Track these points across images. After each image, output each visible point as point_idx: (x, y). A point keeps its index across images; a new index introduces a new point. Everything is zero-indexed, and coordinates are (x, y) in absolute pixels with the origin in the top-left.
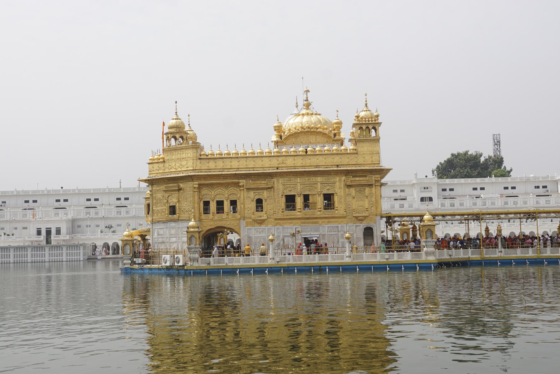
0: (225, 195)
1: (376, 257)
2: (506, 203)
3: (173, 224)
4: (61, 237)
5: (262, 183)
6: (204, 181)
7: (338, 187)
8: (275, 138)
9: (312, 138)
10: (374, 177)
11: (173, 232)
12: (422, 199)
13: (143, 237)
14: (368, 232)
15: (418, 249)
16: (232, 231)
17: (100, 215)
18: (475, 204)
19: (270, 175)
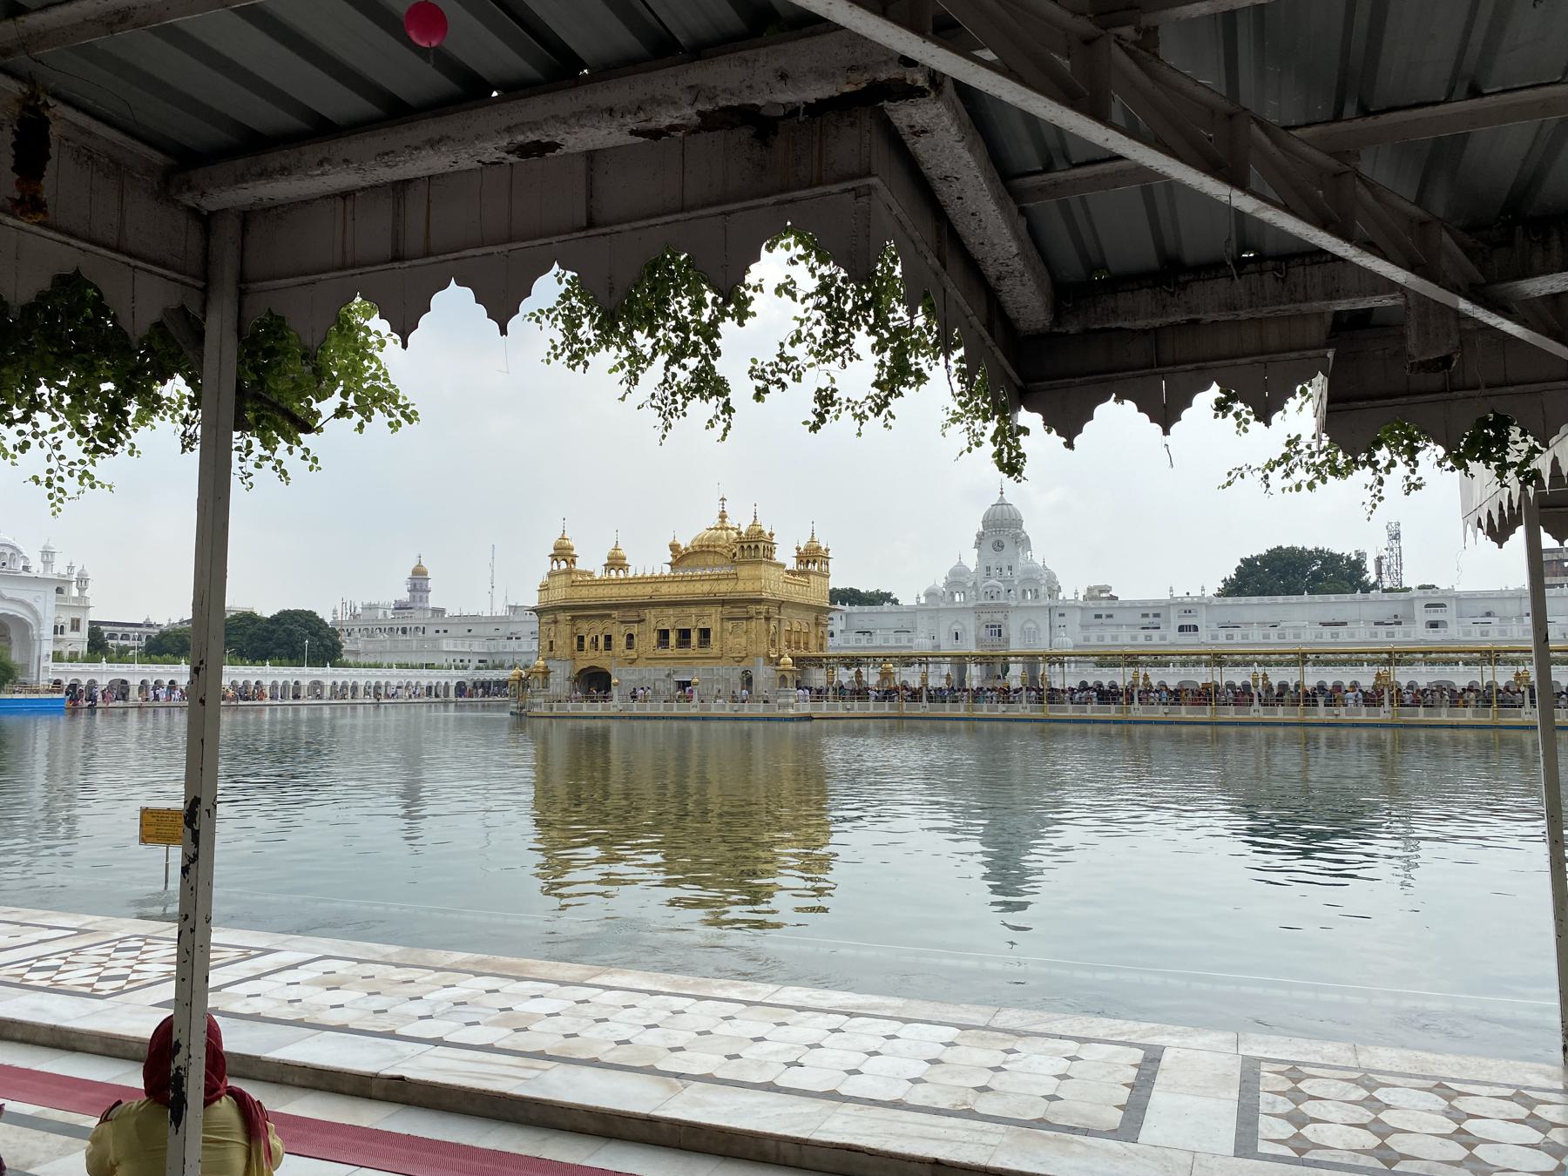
0: (598, 628)
1: (723, 707)
6: (578, 611)
8: (670, 559)
9: (710, 559)
10: (753, 609)
12: (1181, 629)
18: (1266, 637)
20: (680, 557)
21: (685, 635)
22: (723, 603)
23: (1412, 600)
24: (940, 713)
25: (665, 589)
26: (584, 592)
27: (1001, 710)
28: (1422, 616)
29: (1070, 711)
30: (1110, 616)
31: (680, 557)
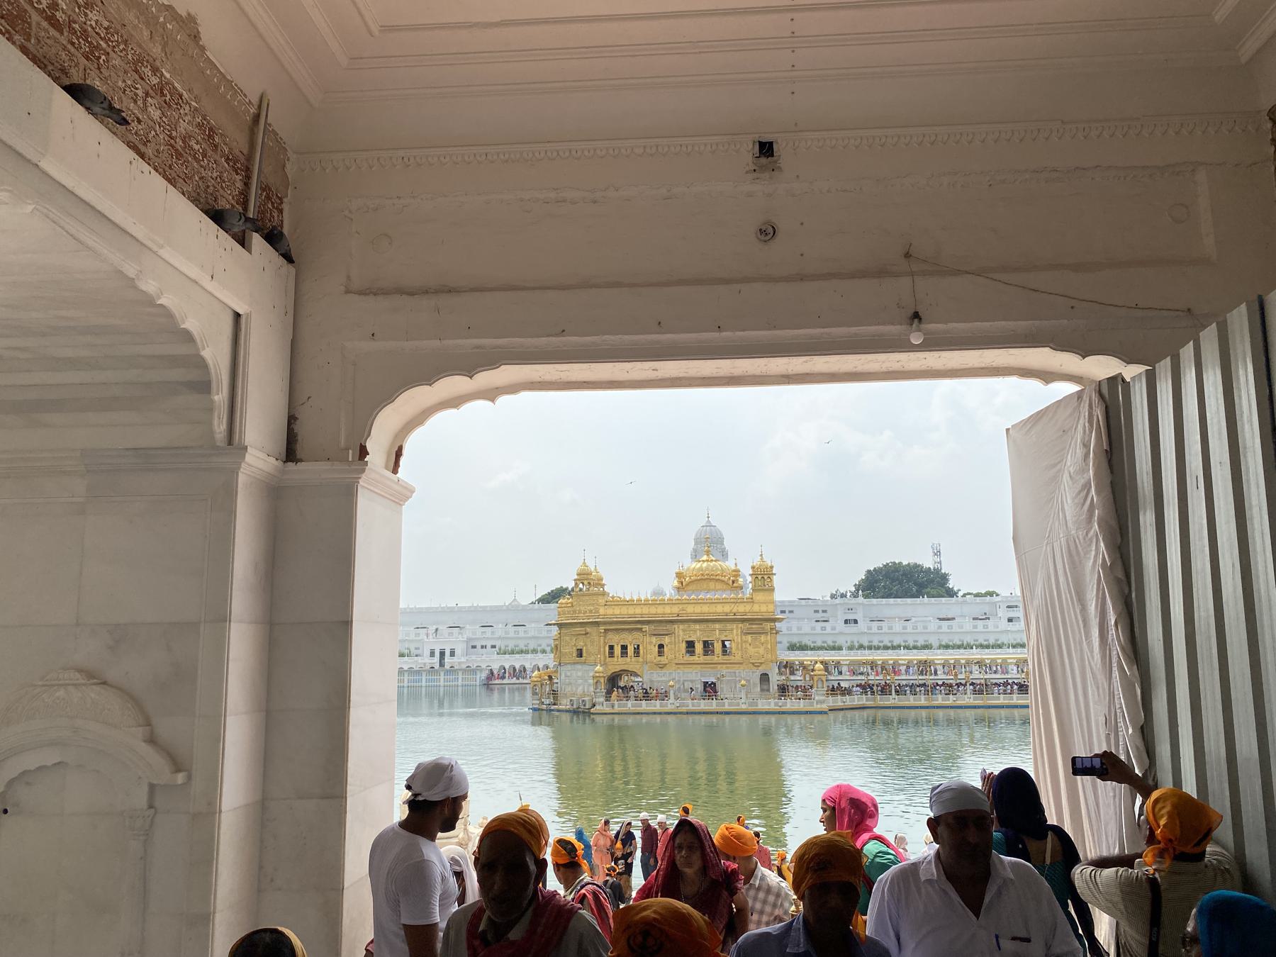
2: (940, 627)
3: (579, 667)
4: (455, 659)
5: (662, 629)
7: (734, 635)
9: (712, 585)
10: (768, 626)
11: (580, 674)
12: (846, 622)
13: (550, 678)
14: (765, 678)
15: (807, 697)
16: (636, 675)
17: (496, 636)
18: (905, 628)
19: (671, 622)
20: (684, 582)
21: (707, 645)
22: (743, 621)
23: (995, 603)
24: (906, 703)
25: (690, 609)
26: (617, 611)
27: (951, 700)
28: (1003, 614)
29: (1002, 700)
30: (791, 612)
31: (684, 582)
